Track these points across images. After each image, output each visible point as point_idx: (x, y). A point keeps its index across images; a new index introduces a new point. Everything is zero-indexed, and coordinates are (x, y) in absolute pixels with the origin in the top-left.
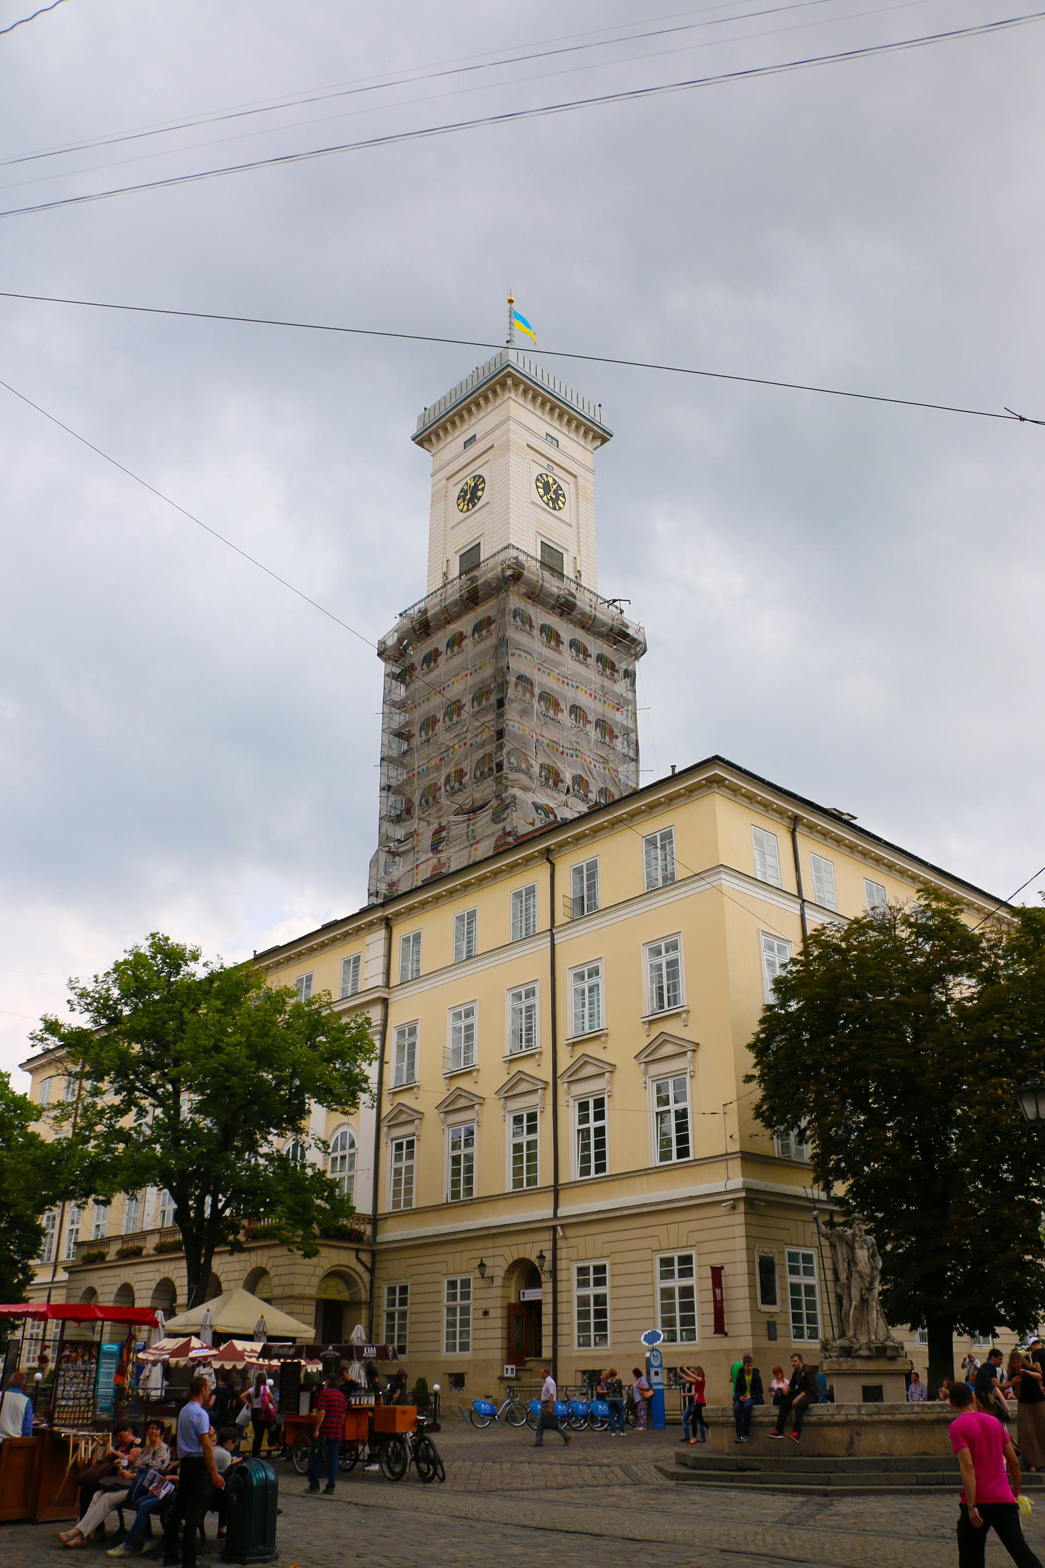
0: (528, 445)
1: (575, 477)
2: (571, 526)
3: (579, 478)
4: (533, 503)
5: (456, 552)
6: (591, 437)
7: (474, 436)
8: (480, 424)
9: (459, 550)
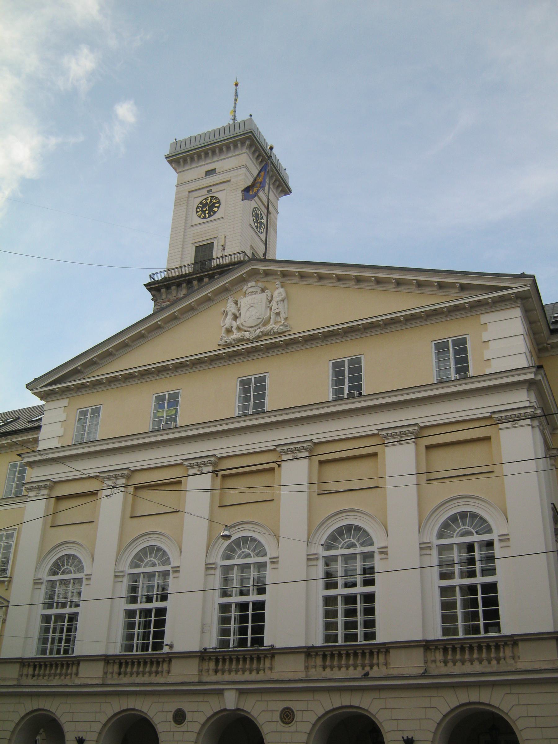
4: (251, 225)
6: (280, 189)
7: (215, 170)
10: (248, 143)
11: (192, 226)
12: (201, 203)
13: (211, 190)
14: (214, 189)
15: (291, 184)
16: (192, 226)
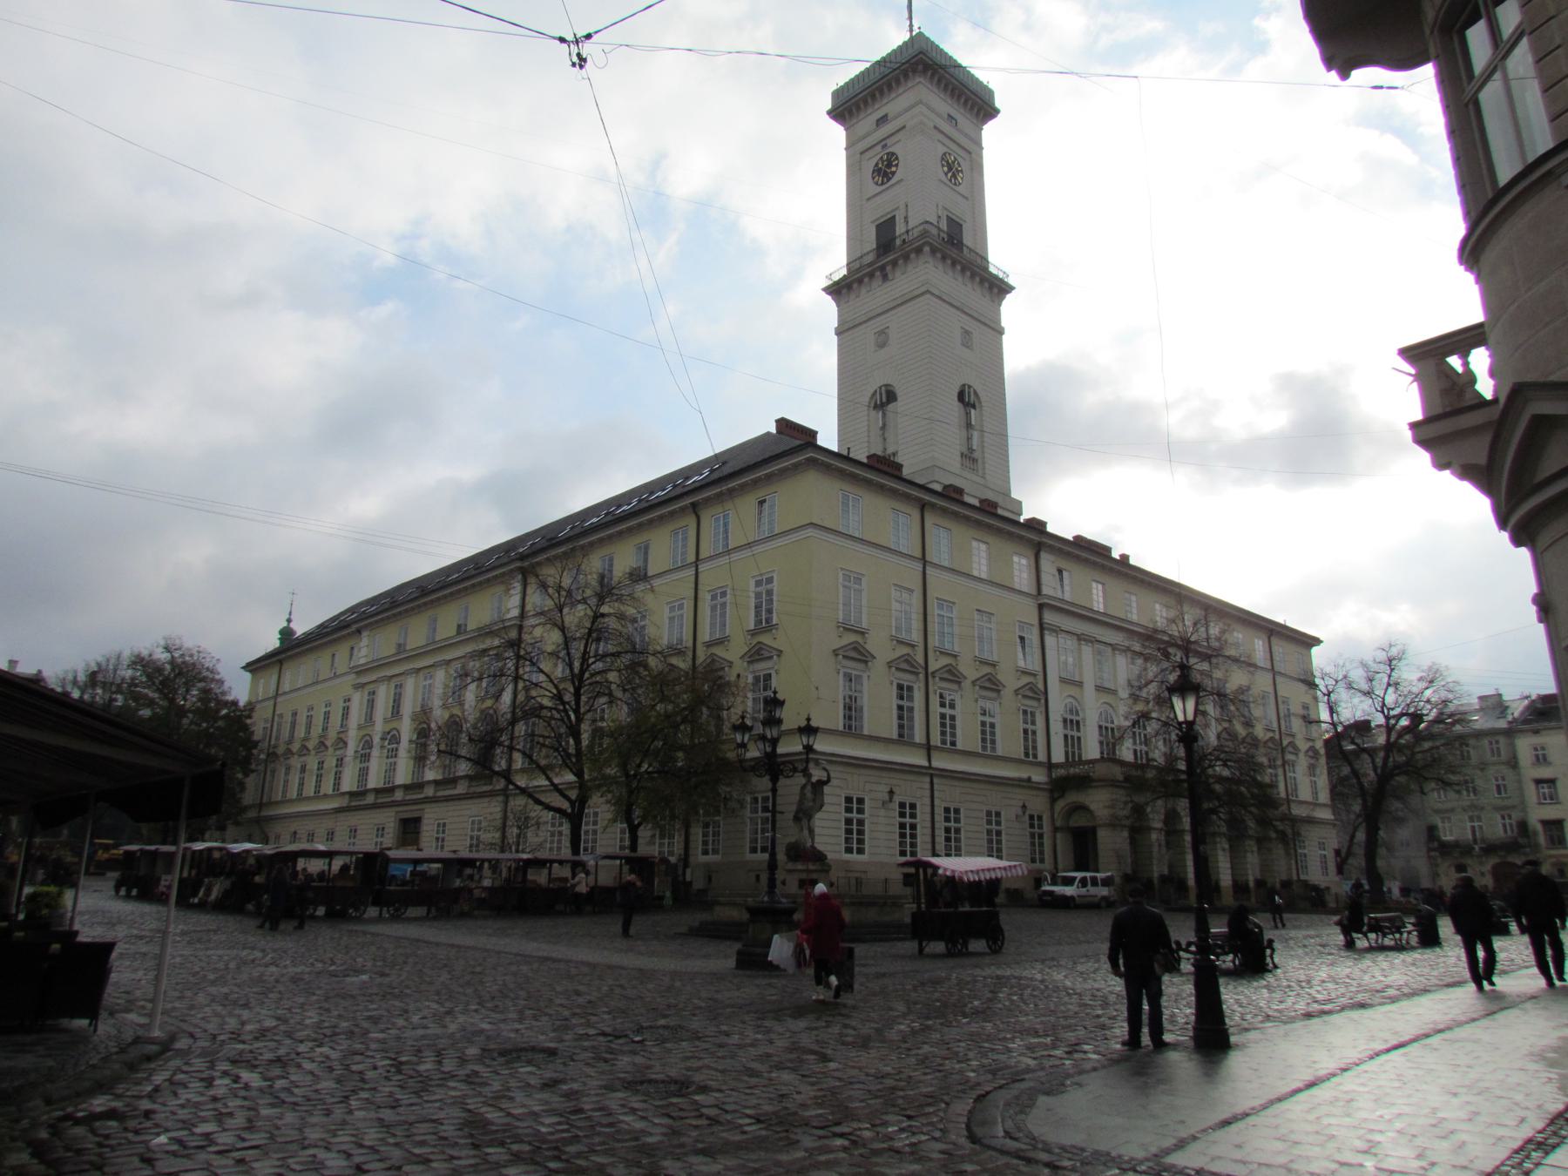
0: (935, 127)
1: (970, 153)
2: (966, 198)
3: (973, 155)
5: (872, 222)
7: (886, 115)
8: (895, 104)
9: (878, 219)
10: (920, 67)
11: (869, 199)
12: (877, 165)
13: (886, 145)
14: (889, 142)
15: (998, 104)
16: (869, 199)
